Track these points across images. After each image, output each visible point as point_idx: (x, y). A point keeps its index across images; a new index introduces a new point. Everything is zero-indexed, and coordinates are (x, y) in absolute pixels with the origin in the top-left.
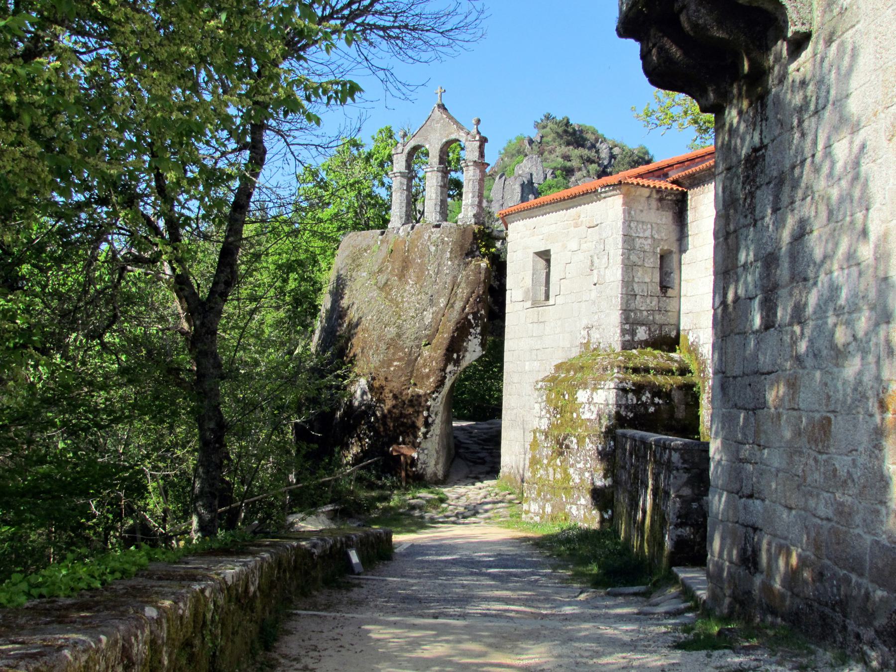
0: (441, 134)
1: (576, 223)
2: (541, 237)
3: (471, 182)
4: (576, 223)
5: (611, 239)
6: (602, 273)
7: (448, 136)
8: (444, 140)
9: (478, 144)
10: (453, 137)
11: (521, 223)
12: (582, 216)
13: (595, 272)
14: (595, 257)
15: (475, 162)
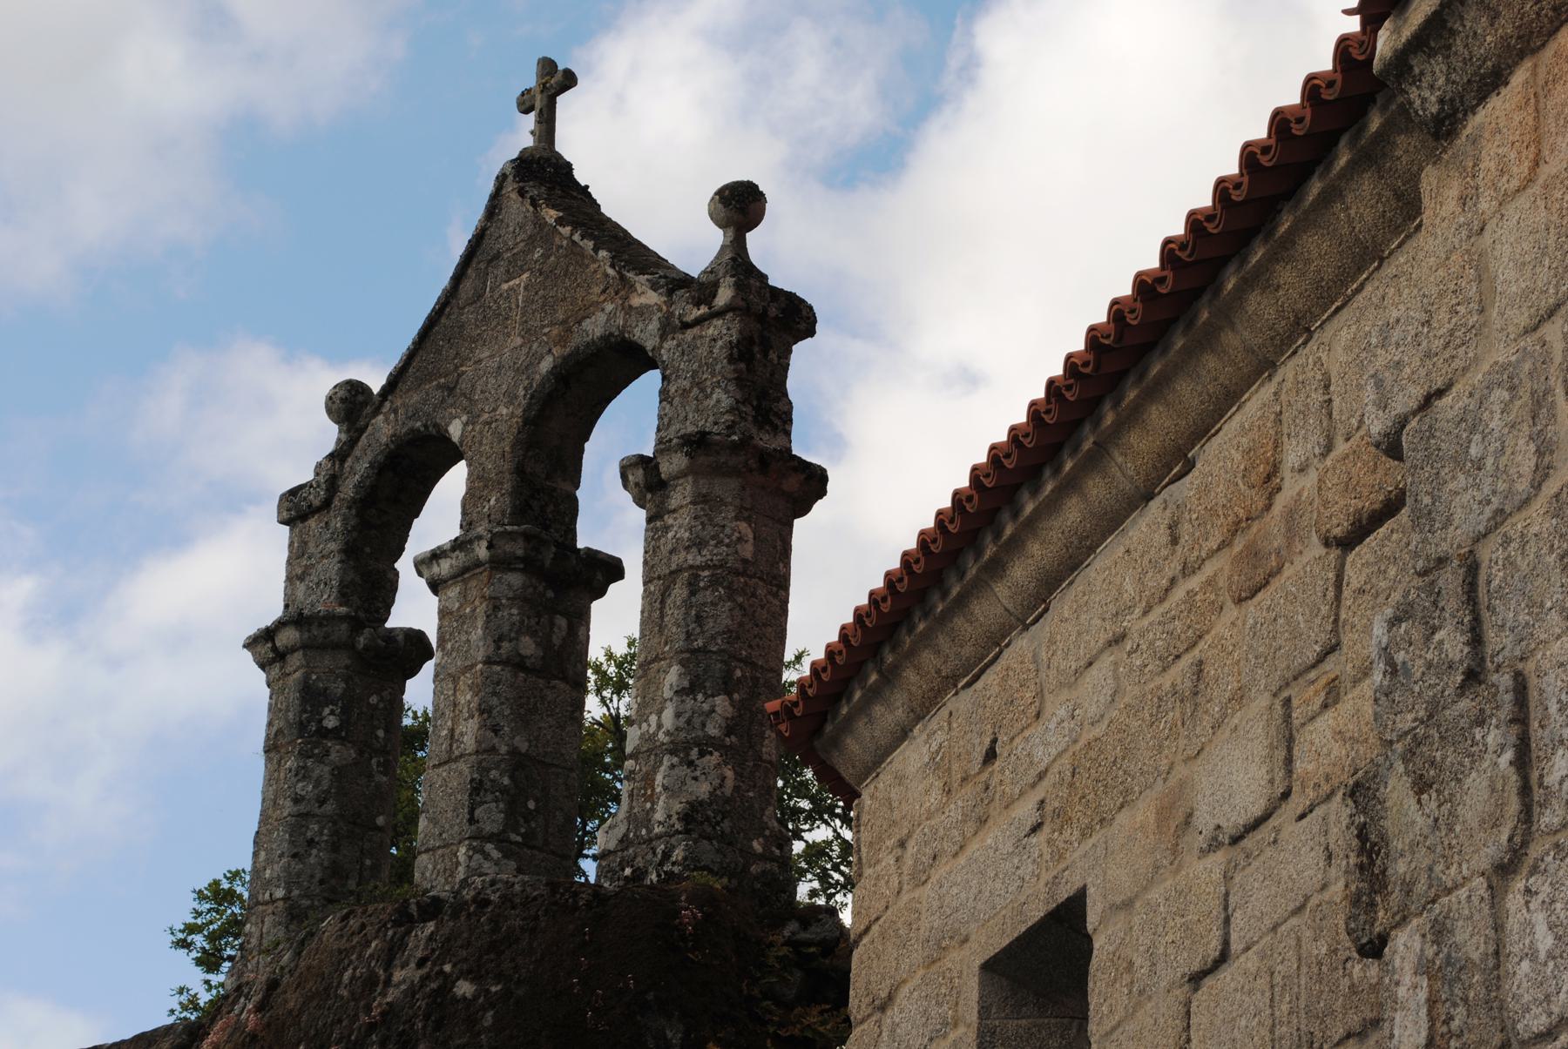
0: (529, 334)
1: (1253, 554)
2: (1025, 811)
3: (679, 592)
4: (1253, 554)
5: (1536, 519)
6: (1471, 941)
7: (562, 340)
8: (546, 365)
9: (722, 332)
10: (594, 327)
11: (912, 756)
12: (1292, 456)
13: (1406, 945)
14: (1396, 788)
15: (697, 443)
